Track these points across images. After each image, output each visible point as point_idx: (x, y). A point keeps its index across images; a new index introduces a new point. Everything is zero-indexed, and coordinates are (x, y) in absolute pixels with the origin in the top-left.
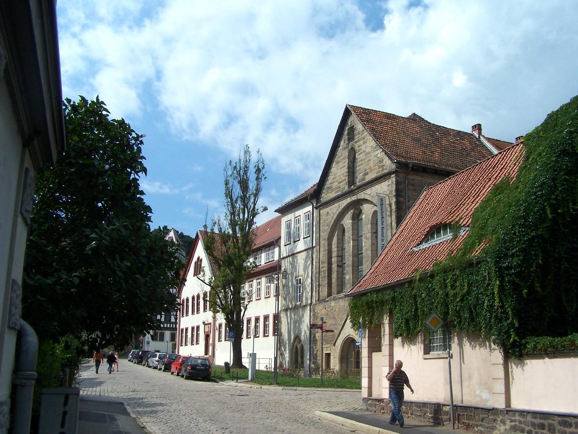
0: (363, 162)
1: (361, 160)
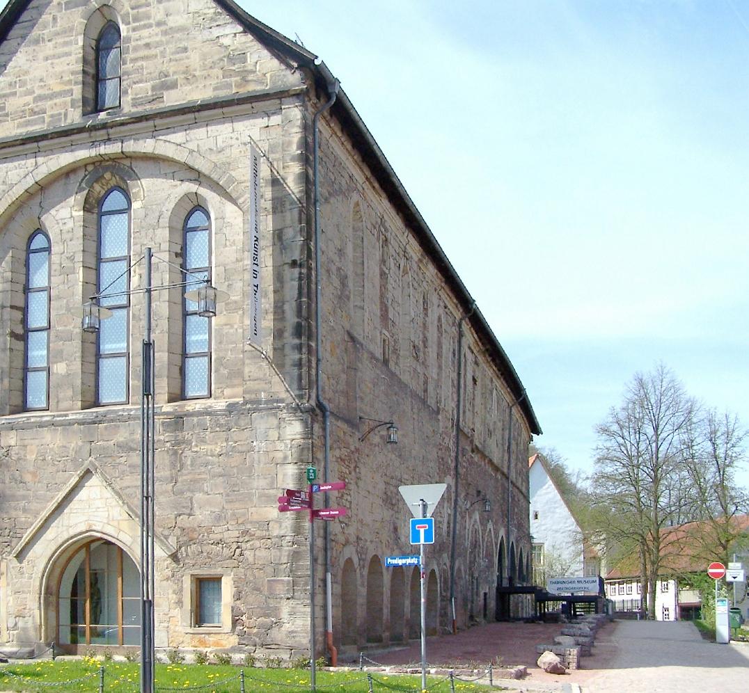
0: (153, 52)
1: (147, 45)
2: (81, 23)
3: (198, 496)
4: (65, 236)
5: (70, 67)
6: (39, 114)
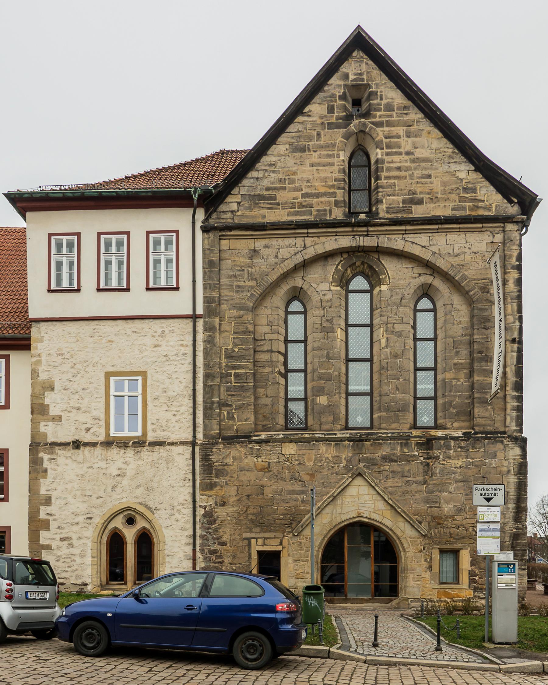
0: (403, 173)
1: (399, 168)
2: (341, 142)
3: (445, 494)
4: (324, 304)
5: (334, 175)
6: (307, 207)
